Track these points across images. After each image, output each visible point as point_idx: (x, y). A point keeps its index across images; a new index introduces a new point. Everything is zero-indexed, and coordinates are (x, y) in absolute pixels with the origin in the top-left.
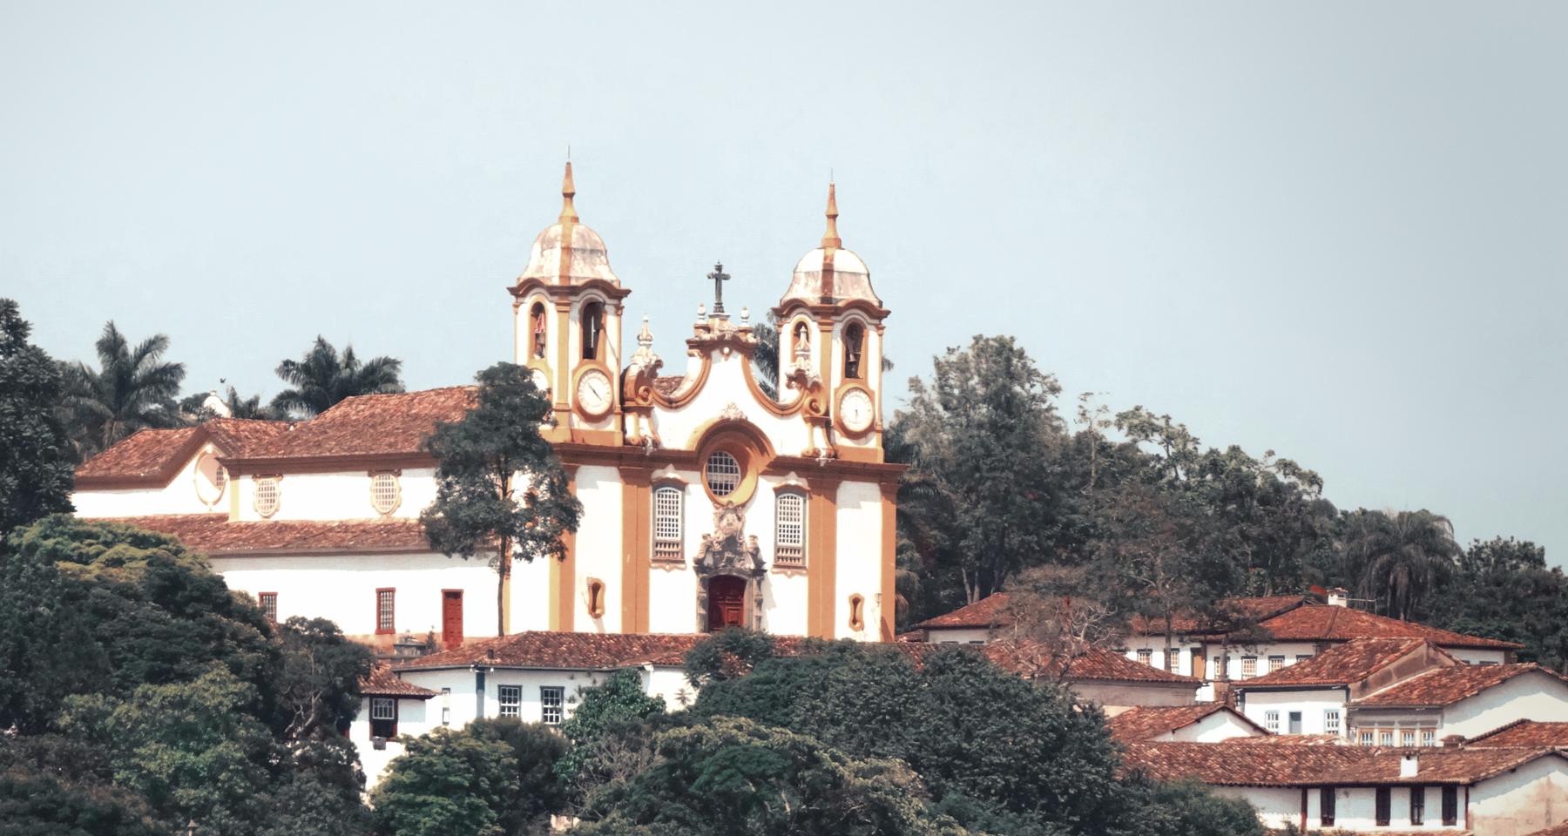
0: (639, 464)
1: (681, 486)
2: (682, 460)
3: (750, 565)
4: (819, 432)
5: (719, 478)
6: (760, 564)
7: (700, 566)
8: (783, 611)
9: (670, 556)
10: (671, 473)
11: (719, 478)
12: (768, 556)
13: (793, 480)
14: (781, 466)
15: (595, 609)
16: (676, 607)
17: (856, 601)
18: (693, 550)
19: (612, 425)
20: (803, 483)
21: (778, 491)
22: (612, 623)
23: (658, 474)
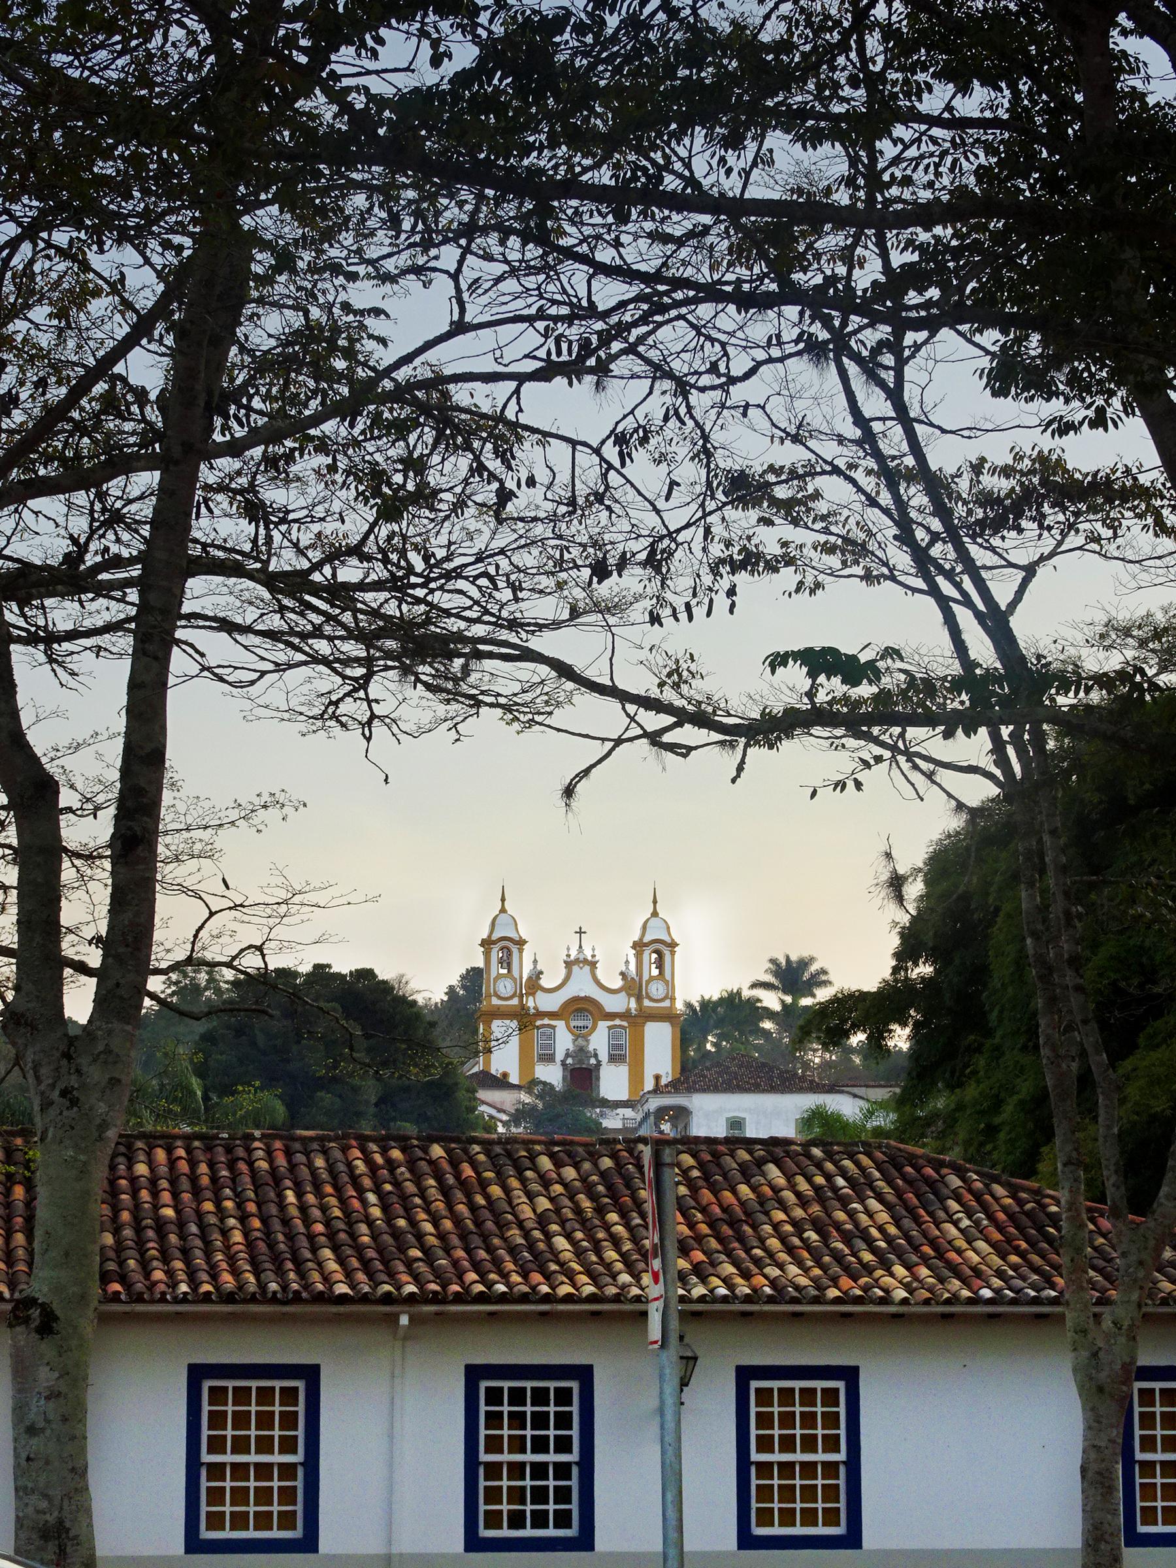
0: (526, 1019)
1: (553, 1027)
2: (552, 1015)
3: (593, 1061)
4: (633, 1000)
7: (563, 1063)
10: (546, 1021)
12: (604, 1056)
13: (617, 1022)
18: (559, 1056)
19: (515, 1001)
21: (610, 1028)
23: (538, 1023)
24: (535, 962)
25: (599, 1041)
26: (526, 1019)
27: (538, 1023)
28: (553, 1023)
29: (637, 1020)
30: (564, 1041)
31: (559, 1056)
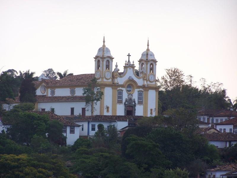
0: (114, 86)
1: (122, 90)
2: (122, 86)
3: (133, 103)
4: (145, 82)
5: (129, 89)
6: (135, 103)
8: (139, 111)
9: (120, 102)
10: (120, 88)
11: (129, 89)
12: (137, 102)
13: (141, 89)
14: (139, 87)
15: (108, 111)
16: (121, 111)
17: (151, 110)
18: (124, 101)
20: (143, 90)
22: (110, 114)
23: (118, 89)
24: (117, 66)
25: (135, 96)
26: (114, 86)
27: (118, 89)
28: (123, 89)
29: (146, 88)
30: (125, 96)
31: (124, 101)
